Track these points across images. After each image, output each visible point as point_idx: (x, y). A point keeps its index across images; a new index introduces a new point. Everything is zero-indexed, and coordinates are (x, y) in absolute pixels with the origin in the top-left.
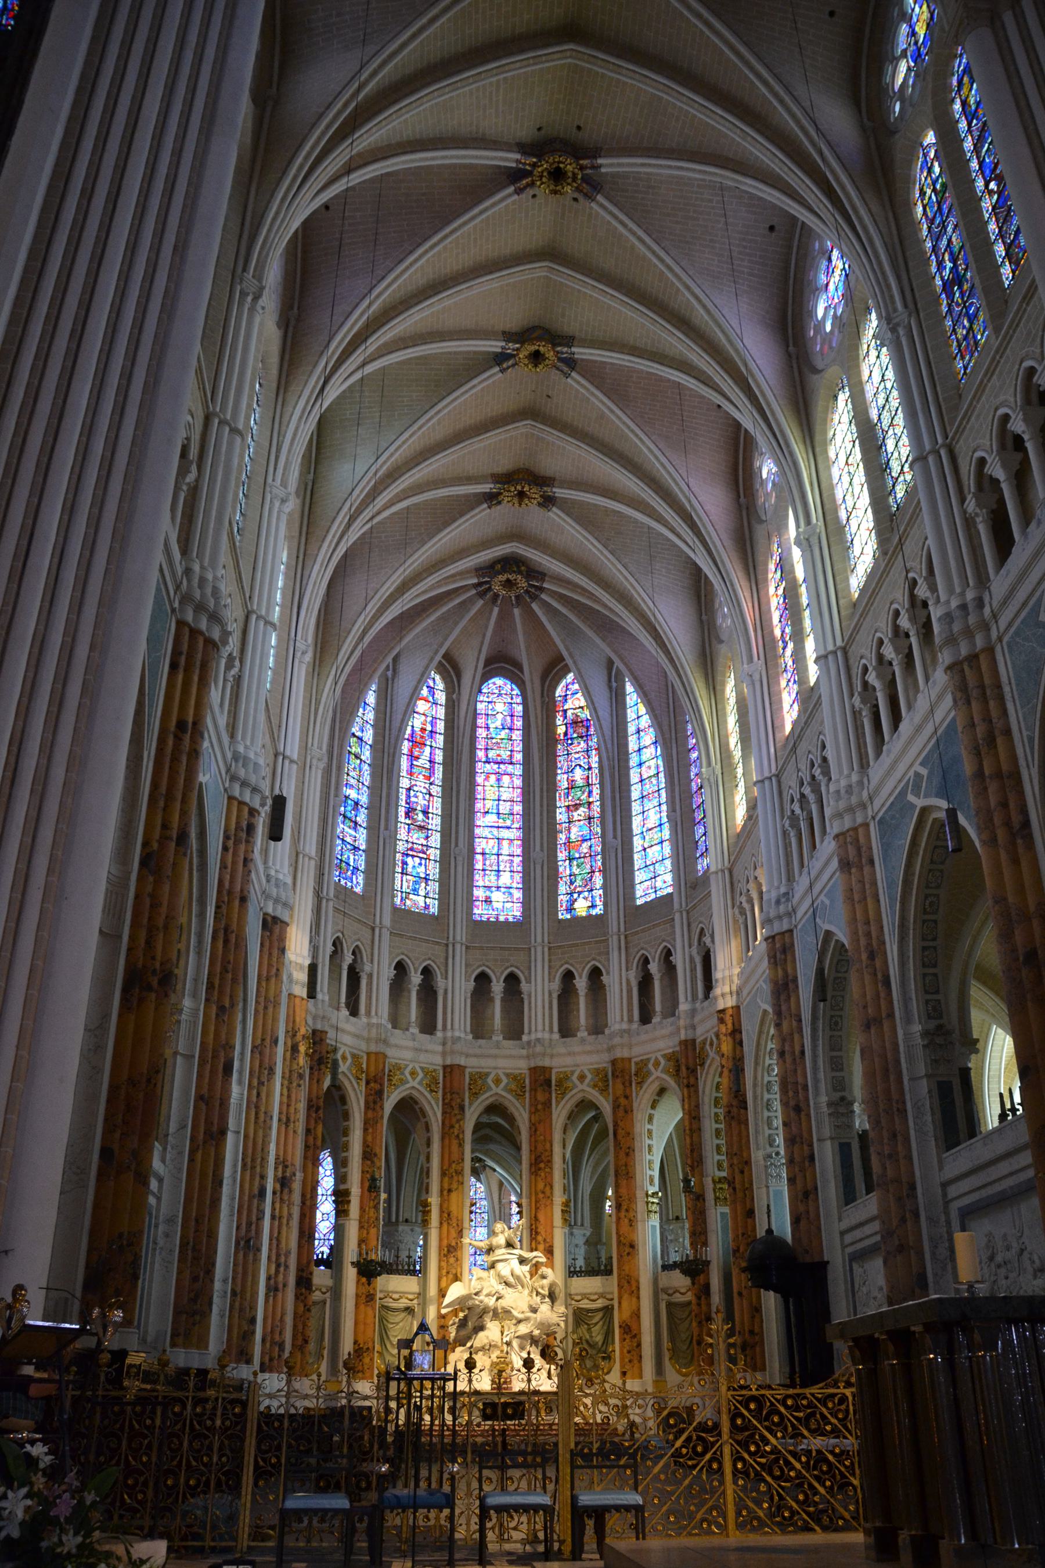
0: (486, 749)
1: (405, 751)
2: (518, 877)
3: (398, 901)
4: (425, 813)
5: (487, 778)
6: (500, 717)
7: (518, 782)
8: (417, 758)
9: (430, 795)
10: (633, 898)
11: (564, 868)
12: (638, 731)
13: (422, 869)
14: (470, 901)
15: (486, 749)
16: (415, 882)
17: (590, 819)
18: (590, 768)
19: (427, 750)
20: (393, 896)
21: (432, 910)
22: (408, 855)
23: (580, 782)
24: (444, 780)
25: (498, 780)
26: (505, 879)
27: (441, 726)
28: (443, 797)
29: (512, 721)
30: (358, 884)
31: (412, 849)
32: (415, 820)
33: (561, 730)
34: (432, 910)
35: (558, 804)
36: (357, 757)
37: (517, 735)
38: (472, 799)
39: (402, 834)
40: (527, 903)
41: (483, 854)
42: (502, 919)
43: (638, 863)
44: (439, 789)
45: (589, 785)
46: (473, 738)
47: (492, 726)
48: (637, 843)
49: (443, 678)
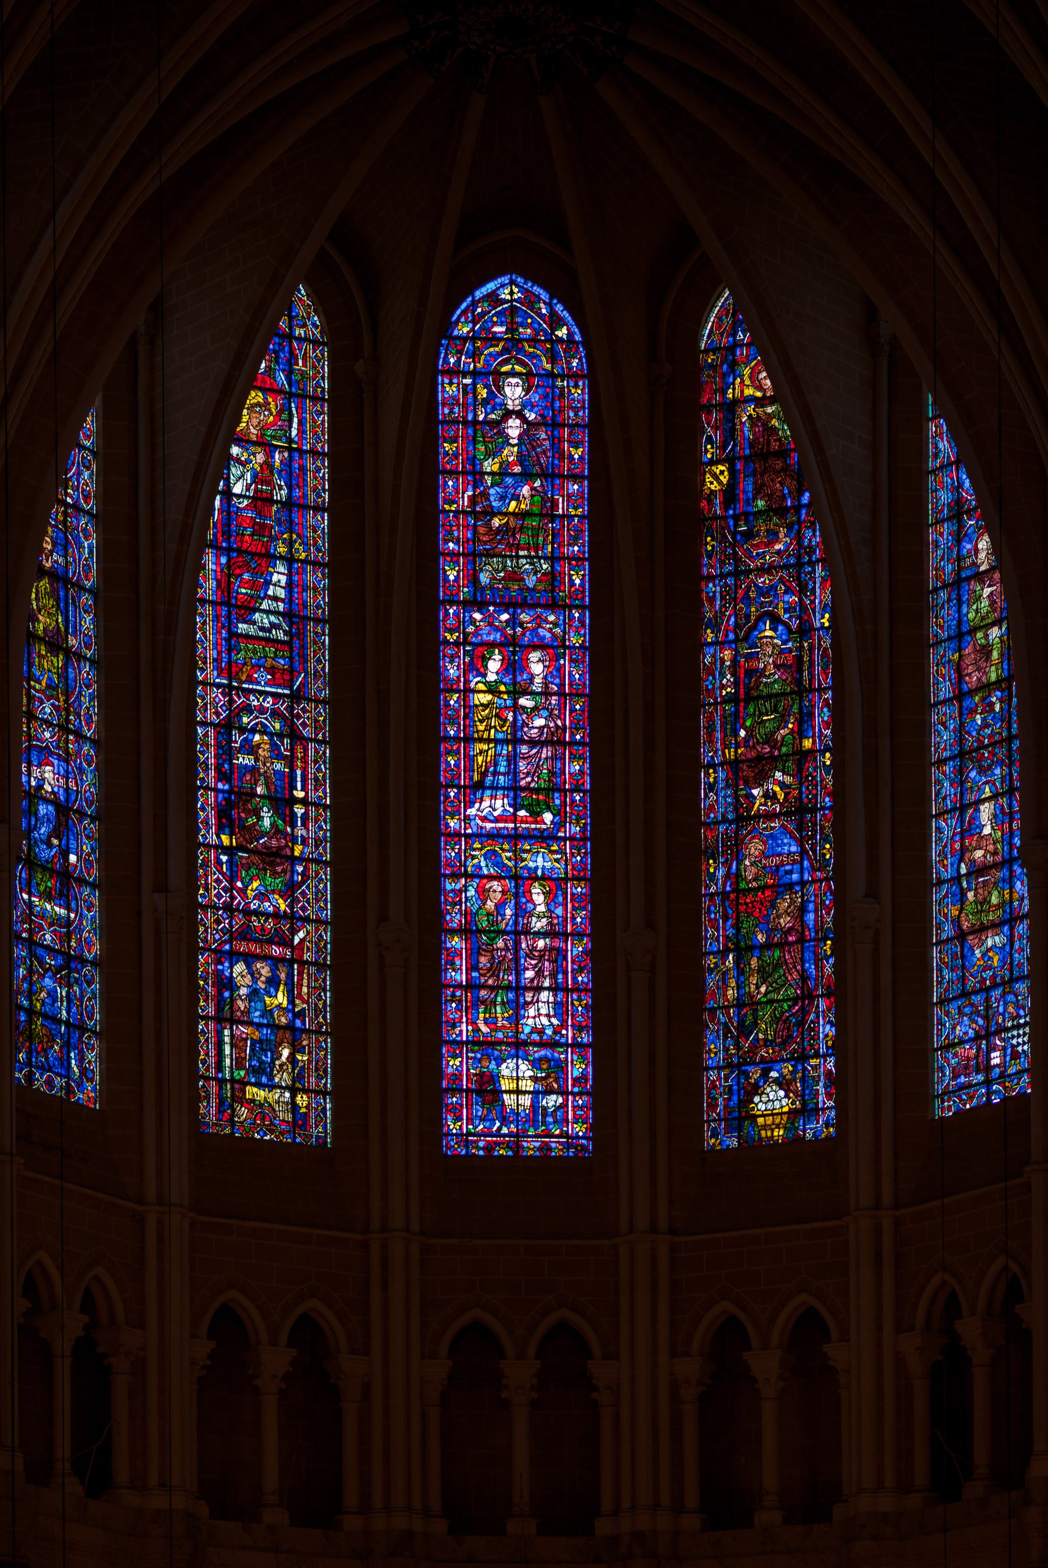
0: (473, 557)
1: (209, 587)
2: (579, 1005)
3: (209, 1110)
4: (283, 803)
5: (477, 666)
6: (514, 428)
7: (575, 673)
8: (247, 610)
9: (296, 737)
10: (924, 1095)
11: (724, 983)
12: (958, 511)
13: (281, 998)
14: (430, 1093)
15: (473, 557)
16: (261, 1045)
17: (799, 811)
18: (805, 630)
19: (279, 575)
20: (195, 1099)
21: (316, 1131)
22: (234, 956)
23: (774, 679)
24: (335, 680)
25: (514, 666)
26: (539, 1014)
27: (318, 476)
28: (333, 742)
29: (556, 443)
30: (83, 1075)
31: (245, 934)
32: (253, 832)
33: (716, 479)
34: (316, 1131)
35: (706, 755)
36: (55, 643)
37: (571, 499)
38: (427, 741)
39: (213, 887)
40: (604, 1095)
41: (468, 931)
42: (531, 1146)
43: (942, 978)
44: (323, 713)
45: (801, 691)
46: (427, 517)
47: (490, 465)
48: (944, 913)
49: (321, 301)
